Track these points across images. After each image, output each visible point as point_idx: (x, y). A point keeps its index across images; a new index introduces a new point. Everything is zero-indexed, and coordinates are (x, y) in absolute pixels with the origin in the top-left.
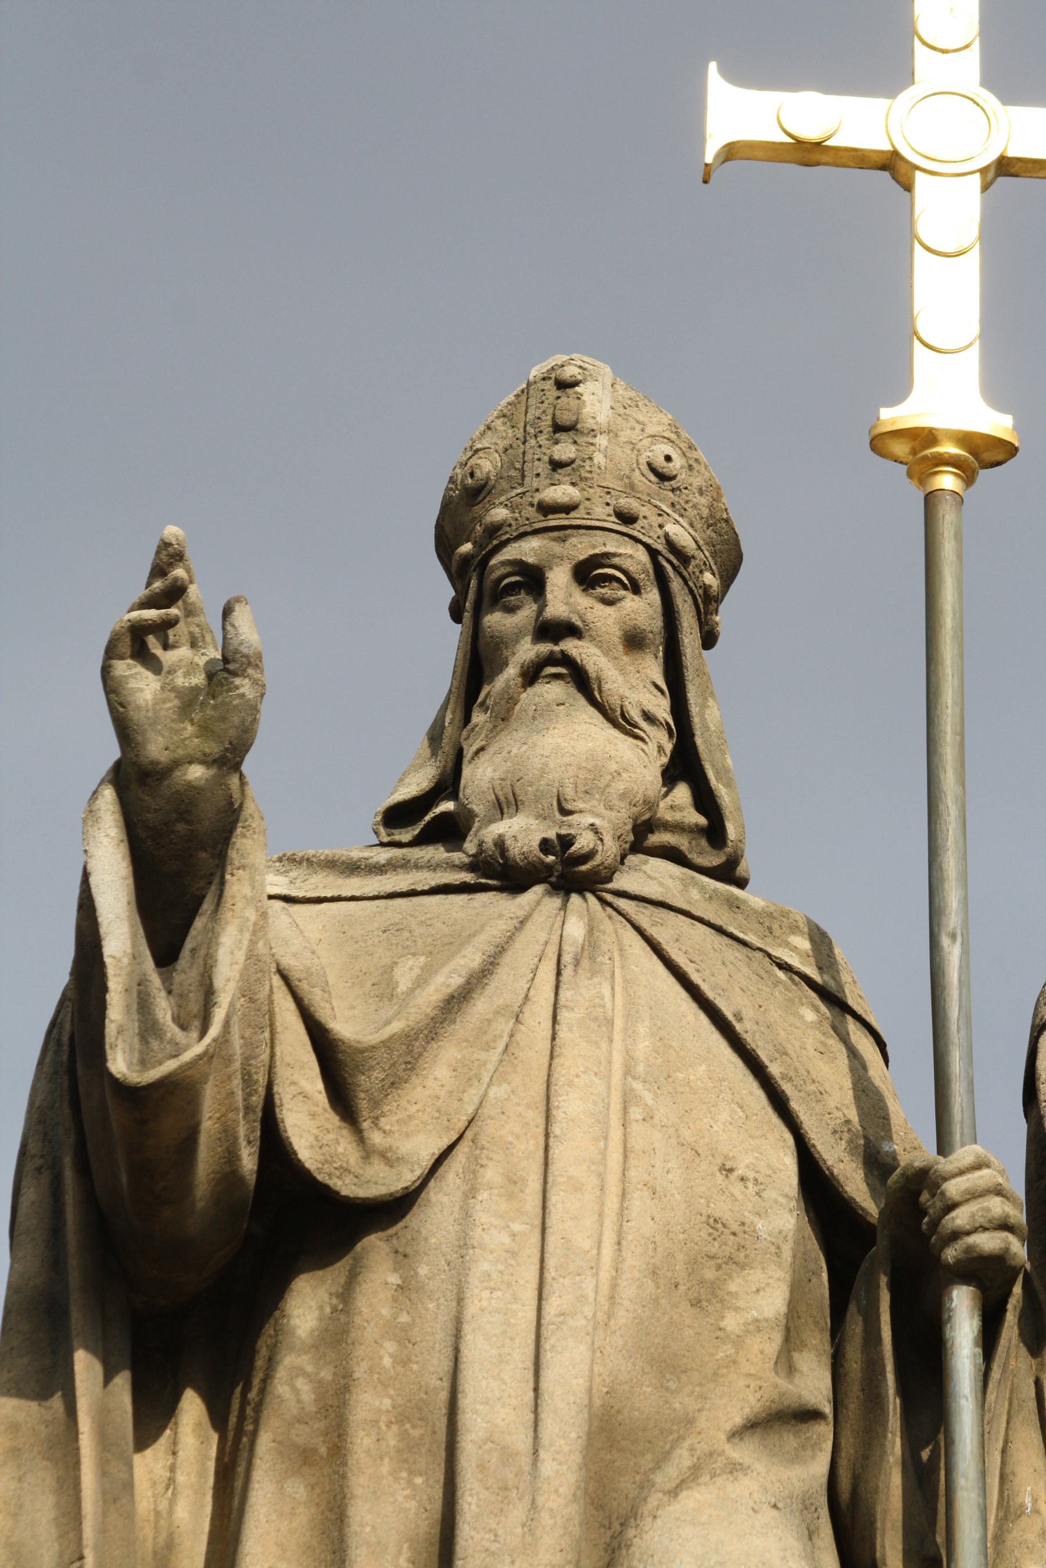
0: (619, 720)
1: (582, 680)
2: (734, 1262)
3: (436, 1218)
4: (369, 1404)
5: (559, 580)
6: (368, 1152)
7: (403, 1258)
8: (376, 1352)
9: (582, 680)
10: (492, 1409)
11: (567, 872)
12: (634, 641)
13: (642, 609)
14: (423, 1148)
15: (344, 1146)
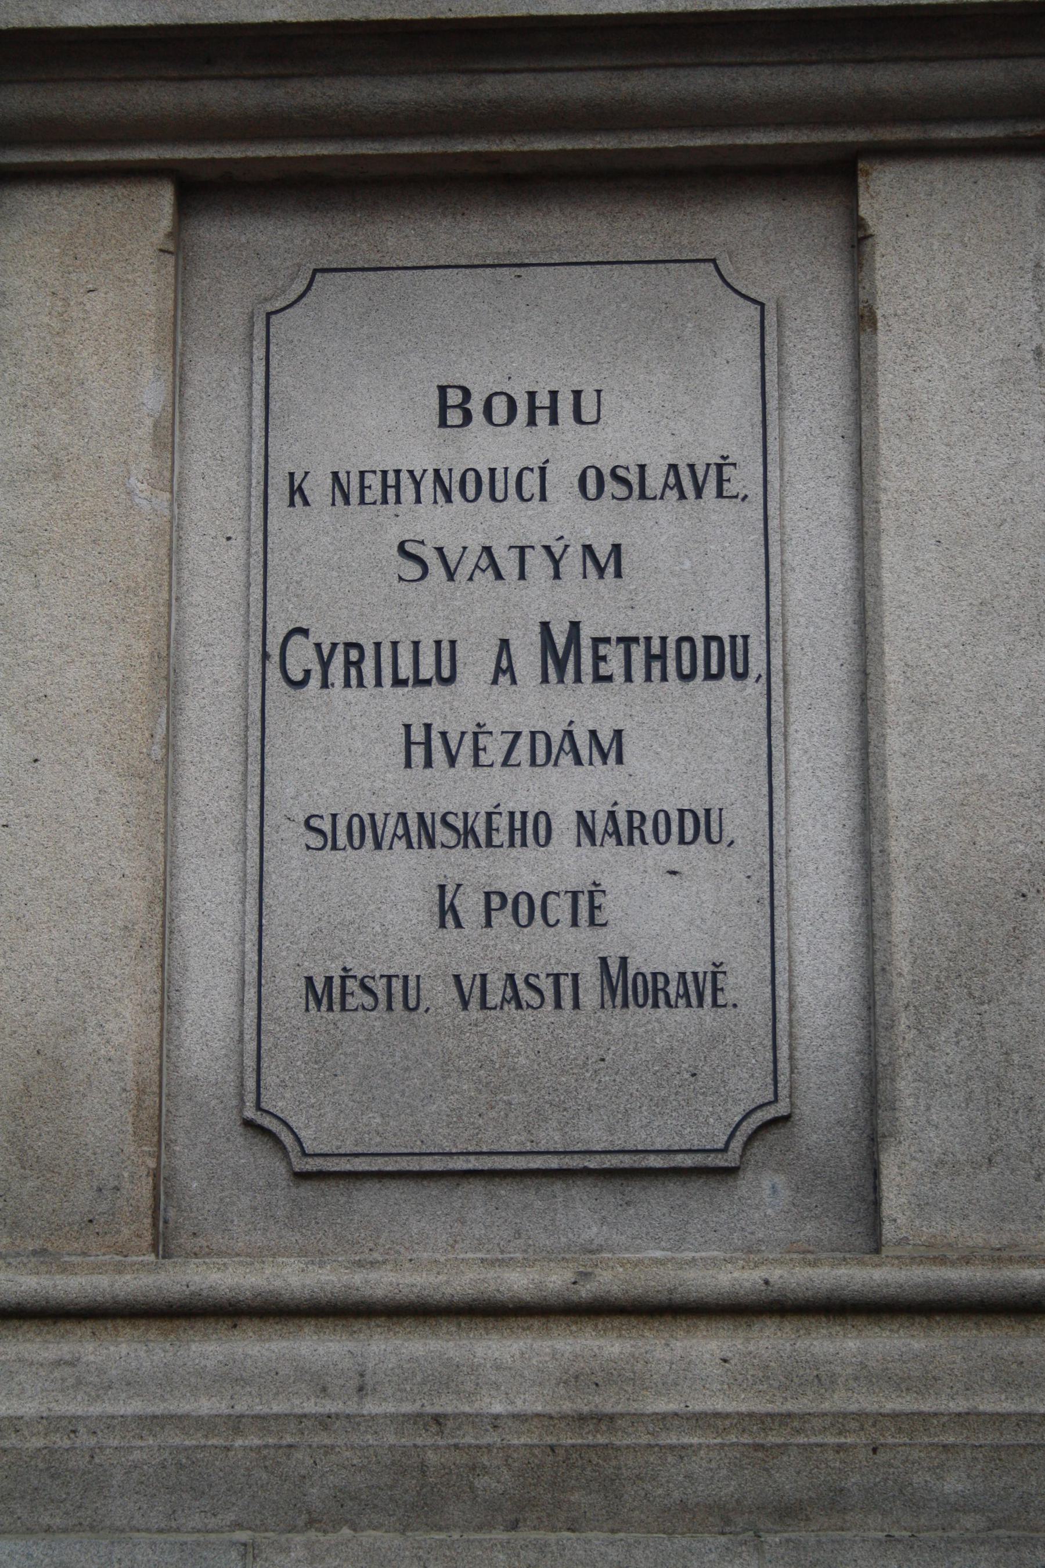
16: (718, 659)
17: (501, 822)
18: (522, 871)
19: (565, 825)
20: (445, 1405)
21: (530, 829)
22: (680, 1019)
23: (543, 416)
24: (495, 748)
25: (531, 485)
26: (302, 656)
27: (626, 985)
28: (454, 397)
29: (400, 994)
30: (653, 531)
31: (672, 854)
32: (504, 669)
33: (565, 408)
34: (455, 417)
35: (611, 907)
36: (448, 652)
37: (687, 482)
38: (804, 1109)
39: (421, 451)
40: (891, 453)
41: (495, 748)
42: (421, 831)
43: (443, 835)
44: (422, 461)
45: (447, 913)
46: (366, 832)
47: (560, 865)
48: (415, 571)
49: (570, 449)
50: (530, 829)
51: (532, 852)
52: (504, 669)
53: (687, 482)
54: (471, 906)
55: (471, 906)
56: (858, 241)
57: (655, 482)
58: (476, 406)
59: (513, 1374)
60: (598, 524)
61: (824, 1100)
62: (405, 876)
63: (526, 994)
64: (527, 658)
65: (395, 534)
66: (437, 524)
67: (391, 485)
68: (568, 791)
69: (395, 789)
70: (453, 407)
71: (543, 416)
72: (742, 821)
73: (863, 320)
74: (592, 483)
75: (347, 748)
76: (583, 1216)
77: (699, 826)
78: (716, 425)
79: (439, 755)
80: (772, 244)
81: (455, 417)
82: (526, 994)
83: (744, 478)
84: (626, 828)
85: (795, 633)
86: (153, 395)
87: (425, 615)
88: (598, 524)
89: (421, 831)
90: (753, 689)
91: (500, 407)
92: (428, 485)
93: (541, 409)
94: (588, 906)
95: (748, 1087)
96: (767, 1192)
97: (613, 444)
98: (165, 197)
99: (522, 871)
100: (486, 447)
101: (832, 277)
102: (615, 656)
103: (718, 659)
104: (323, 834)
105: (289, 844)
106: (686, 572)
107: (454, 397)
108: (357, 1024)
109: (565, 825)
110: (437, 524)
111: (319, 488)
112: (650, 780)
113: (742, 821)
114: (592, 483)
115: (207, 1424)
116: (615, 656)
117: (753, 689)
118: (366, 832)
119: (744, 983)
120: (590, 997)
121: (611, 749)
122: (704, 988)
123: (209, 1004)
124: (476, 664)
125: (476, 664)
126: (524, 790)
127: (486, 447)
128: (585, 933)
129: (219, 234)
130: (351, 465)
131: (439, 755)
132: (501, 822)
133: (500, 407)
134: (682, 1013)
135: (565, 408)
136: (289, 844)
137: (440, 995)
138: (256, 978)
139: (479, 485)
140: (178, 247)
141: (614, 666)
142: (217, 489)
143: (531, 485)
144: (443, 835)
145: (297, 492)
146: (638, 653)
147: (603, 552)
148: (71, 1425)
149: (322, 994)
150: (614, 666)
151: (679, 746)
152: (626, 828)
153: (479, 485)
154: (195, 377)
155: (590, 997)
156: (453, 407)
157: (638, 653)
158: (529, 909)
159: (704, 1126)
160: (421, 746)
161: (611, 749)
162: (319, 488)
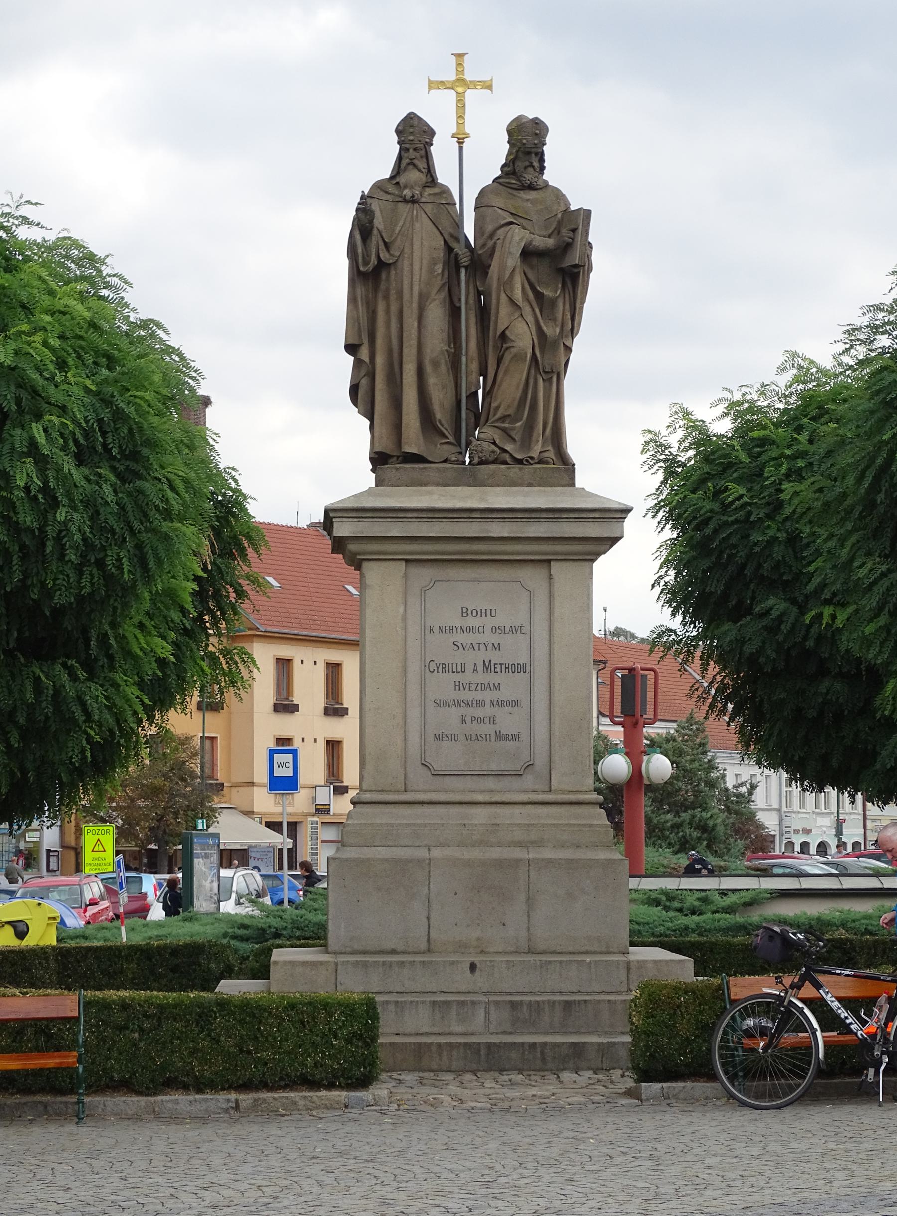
0: (419, 170)
1: (415, 166)
2: (435, 264)
3: (399, 264)
4: (393, 292)
5: (411, 150)
6: (391, 255)
7: (395, 269)
8: (393, 284)
9: (415, 166)
10: (406, 295)
11: (413, 201)
12: (421, 157)
13: (423, 152)
14: (397, 254)
15: (387, 256)
16: (521, 668)
17: (475, 702)
18: (479, 713)
19: (488, 703)
20: (466, 822)
21: (480, 704)
22: (511, 744)
23: (484, 615)
24: (473, 687)
25: (480, 630)
26: (433, 666)
27: (500, 737)
28: (465, 610)
29: (454, 738)
30: (507, 640)
31: (510, 709)
32: (475, 670)
33: (488, 613)
34: (465, 614)
35: (497, 721)
36: (463, 665)
37: (514, 630)
38: (537, 763)
39: (458, 622)
40: (557, 626)
41: (473, 687)
42: (458, 704)
43: (462, 705)
44: (458, 624)
45: (464, 721)
46: (447, 704)
47: (488, 711)
48: (456, 648)
49: (489, 622)
50: (480, 704)
51: (481, 708)
52: (475, 670)
53: (514, 630)
54: (468, 720)
55: (468, 720)
56: (550, 577)
57: (507, 630)
58: (469, 612)
59: (481, 815)
60: (495, 639)
61: (540, 761)
62: (455, 713)
63: (480, 739)
64: (480, 667)
65: (452, 640)
66: (461, 638)
67: (451, 629)
68: (488, 696)
69: (452, 695)
70: (464, 612)
71: (484, 615)
72: (525, 703)
73: (551, 596)
74: (494, 630)
75: (442, 686)
76: (491, 783)
77: (516, 704)
78: (521, 618)
79: (462, 688)
80: (532, 577)
81: (465, 614)
82: (480, 739)
83: (526, 629)
84: (500, 704)
85: (536, 663)
86: (401, 610)
87: (458, 658)
88: (495, 639)
89: (458, 704)
90: (527, 675)
91: (474, 612)
92: (459, 629)
93: (482, 613)
94: (493, 720)
95: (525, 757)
96: (528, 781)
97: (499, 621)
98: (404, 563)
99: (479, 713)
100: (472, 622)
101: (545, 585)
102: (498, 667)
103: (521, 668)
104: (438, 704)
105: (430, 706)
106: (514, 650)
107: (465, 610)
108: (445, 744)
109: (488, 703)
110: (461, 638)
111: (436, 629)
112: (506, 694)
113: (525, 703)
114: (494, 630)
115: (419, 825)
116: (498, 667)
117: (527, 675)
118: (447, 704)
119: (524, 737)
120: (493, 739)
121: (498, 687)
122: (516, 738)
123: (414, 739)
124: (470, 668)
125: (470, 668)
126: (479, 696)
127: (472, 622)
128: (492, 725)
129: (414, 571)
130: (443, 625)
131: (462, 688)
132: (475, 702)
133: (474, 612)
134: (512, 743)
135: (488, 613)
136: (430, 706)
137: (461, 737)
138: (423, 735)
139: (470, 629)
140: (406, 577)
141: (498, 670)
142: (414, 630)
143: (480, 630)
144: (462, 705)
145: (431, 630)
146: (503, 666)
147: (496, 645)
148: (392, 825)
149: (438, 738)
150: (498, 670)
151: (511, 686)
152: (500, 704)
153: (470, 629)
154: (408, 603)
155: (493, 739)
156: (464, 612)
157: (503, 666)
158: (480, 721)
159: (517, 766)
160: (458, 686)
161: (498, 687)
162: (436, 629)
